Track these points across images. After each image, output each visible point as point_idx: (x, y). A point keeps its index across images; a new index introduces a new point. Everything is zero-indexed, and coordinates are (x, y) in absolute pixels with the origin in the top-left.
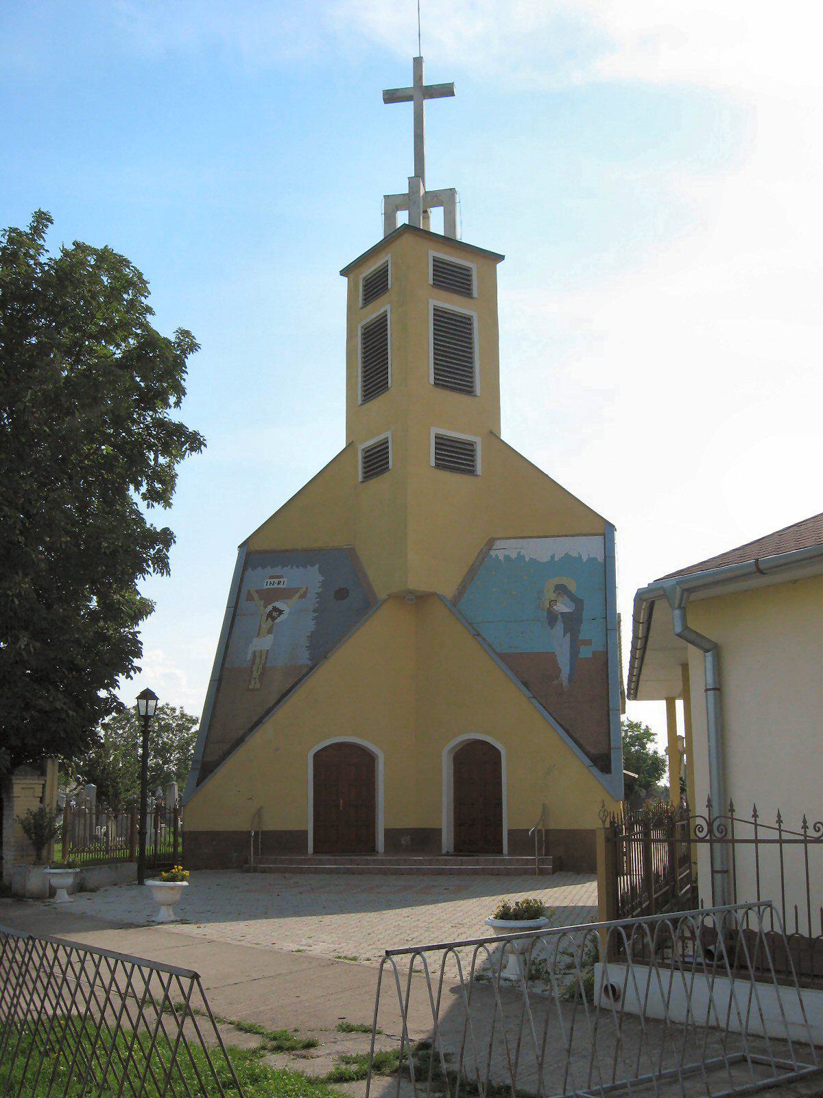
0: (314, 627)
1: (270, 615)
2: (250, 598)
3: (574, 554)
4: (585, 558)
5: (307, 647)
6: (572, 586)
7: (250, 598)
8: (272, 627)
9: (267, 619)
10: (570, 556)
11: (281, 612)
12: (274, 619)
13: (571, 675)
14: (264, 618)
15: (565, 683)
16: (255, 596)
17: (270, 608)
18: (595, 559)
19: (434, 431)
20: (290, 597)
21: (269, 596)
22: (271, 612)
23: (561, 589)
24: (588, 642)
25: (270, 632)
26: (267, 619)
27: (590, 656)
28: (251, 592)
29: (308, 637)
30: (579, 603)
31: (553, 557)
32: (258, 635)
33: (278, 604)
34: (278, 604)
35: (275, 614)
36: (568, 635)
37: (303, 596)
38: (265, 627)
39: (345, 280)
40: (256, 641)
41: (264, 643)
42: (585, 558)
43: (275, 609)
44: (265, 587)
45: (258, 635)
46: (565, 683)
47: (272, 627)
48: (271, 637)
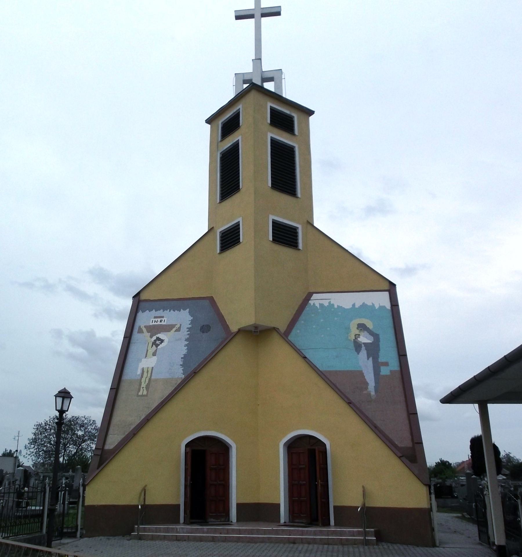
0: (186, 351)
1: (154, 343)
2: (140, 331)
3: (369, 304)
4: (377, 307)
5: (181, 365)
6: (370, 325)
7: (140, 331)
8: (156, 351)
9: (152, 346)
10: (366, 305)
11: (162, 341)
12: (157, 346)
13: (375, 387)
14: (151, 344)
15: (373, 393)
16: (144, 330)
17: (154, 338)
18: (384, 307)
19: (272, 217)
20: (169, 331)
21: (153, 330)
22: (155, 341)
23: (362, 327)
24: (386, 364)
25: (154, 354)
26: (152, 346)
27: (388, 373)
28: (141, 327)
29: (182, 358)
30: (376, 337)
31: (354, 305)
32: (146, 356)
33: (161, 336)
34: (161, 336)
35: (158, 342)
36: (371, 359)
37: (178, 330)
38: (152, 350)
39: (209, 126)
40: (144, 360)
41: (149, 363)
42: (377, 307)
43: (158, 339)
44: (151, 324)
45: (146, 356)
46: (373, 393)
47: (156, 351)
48: (155, 358)
